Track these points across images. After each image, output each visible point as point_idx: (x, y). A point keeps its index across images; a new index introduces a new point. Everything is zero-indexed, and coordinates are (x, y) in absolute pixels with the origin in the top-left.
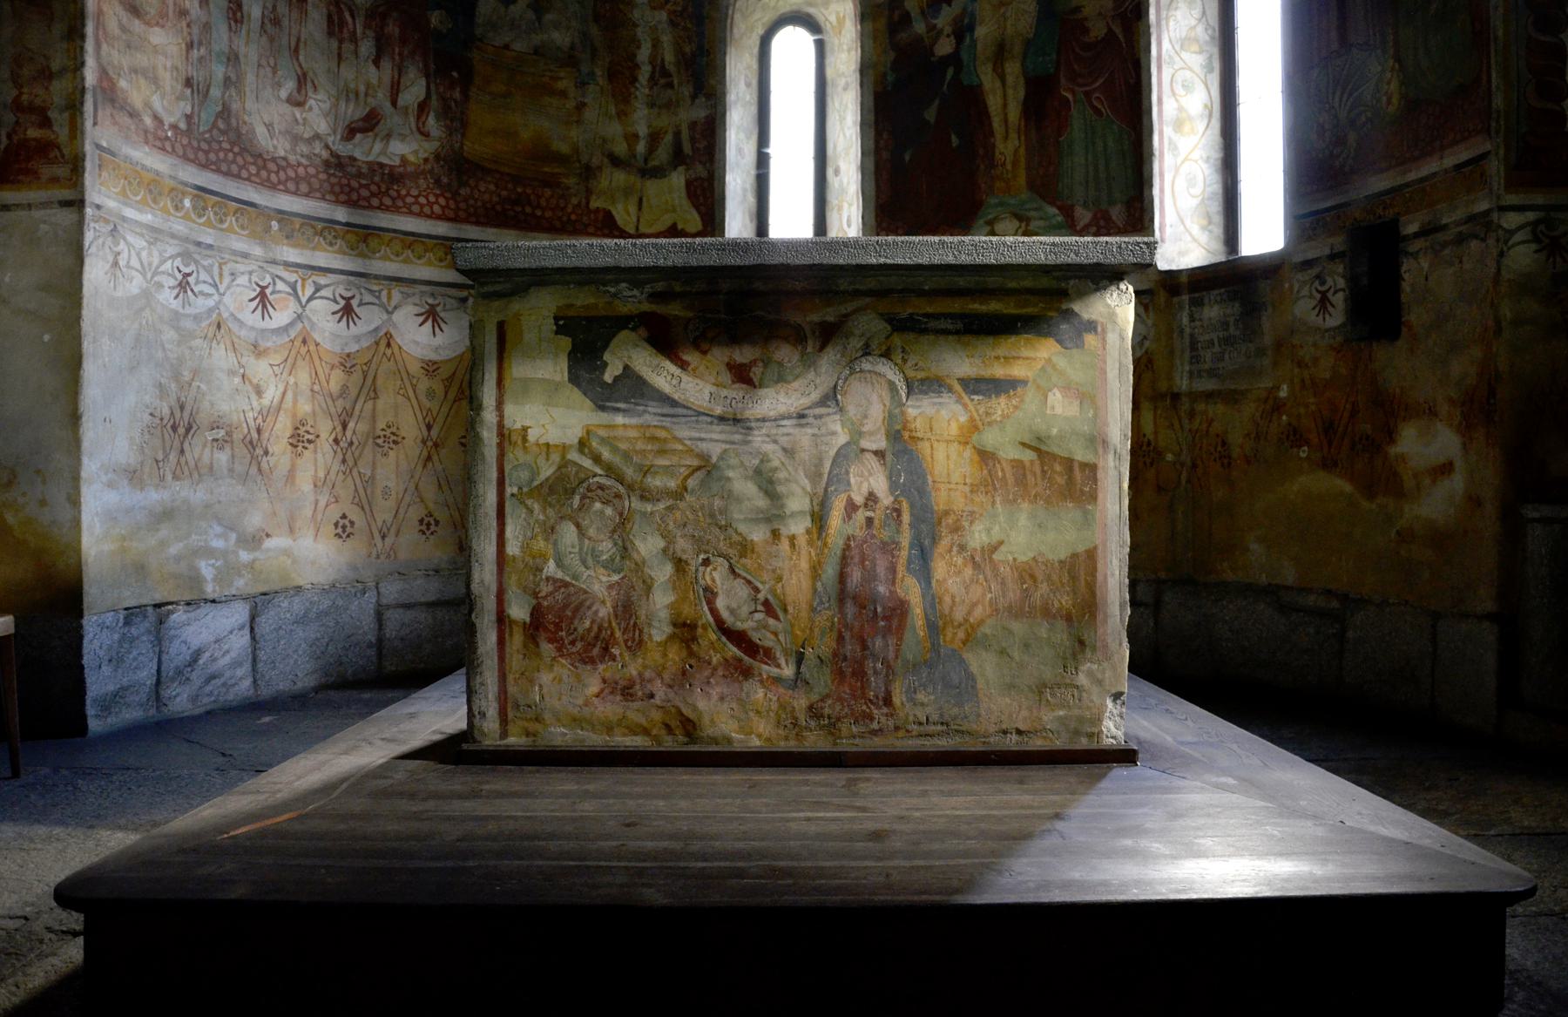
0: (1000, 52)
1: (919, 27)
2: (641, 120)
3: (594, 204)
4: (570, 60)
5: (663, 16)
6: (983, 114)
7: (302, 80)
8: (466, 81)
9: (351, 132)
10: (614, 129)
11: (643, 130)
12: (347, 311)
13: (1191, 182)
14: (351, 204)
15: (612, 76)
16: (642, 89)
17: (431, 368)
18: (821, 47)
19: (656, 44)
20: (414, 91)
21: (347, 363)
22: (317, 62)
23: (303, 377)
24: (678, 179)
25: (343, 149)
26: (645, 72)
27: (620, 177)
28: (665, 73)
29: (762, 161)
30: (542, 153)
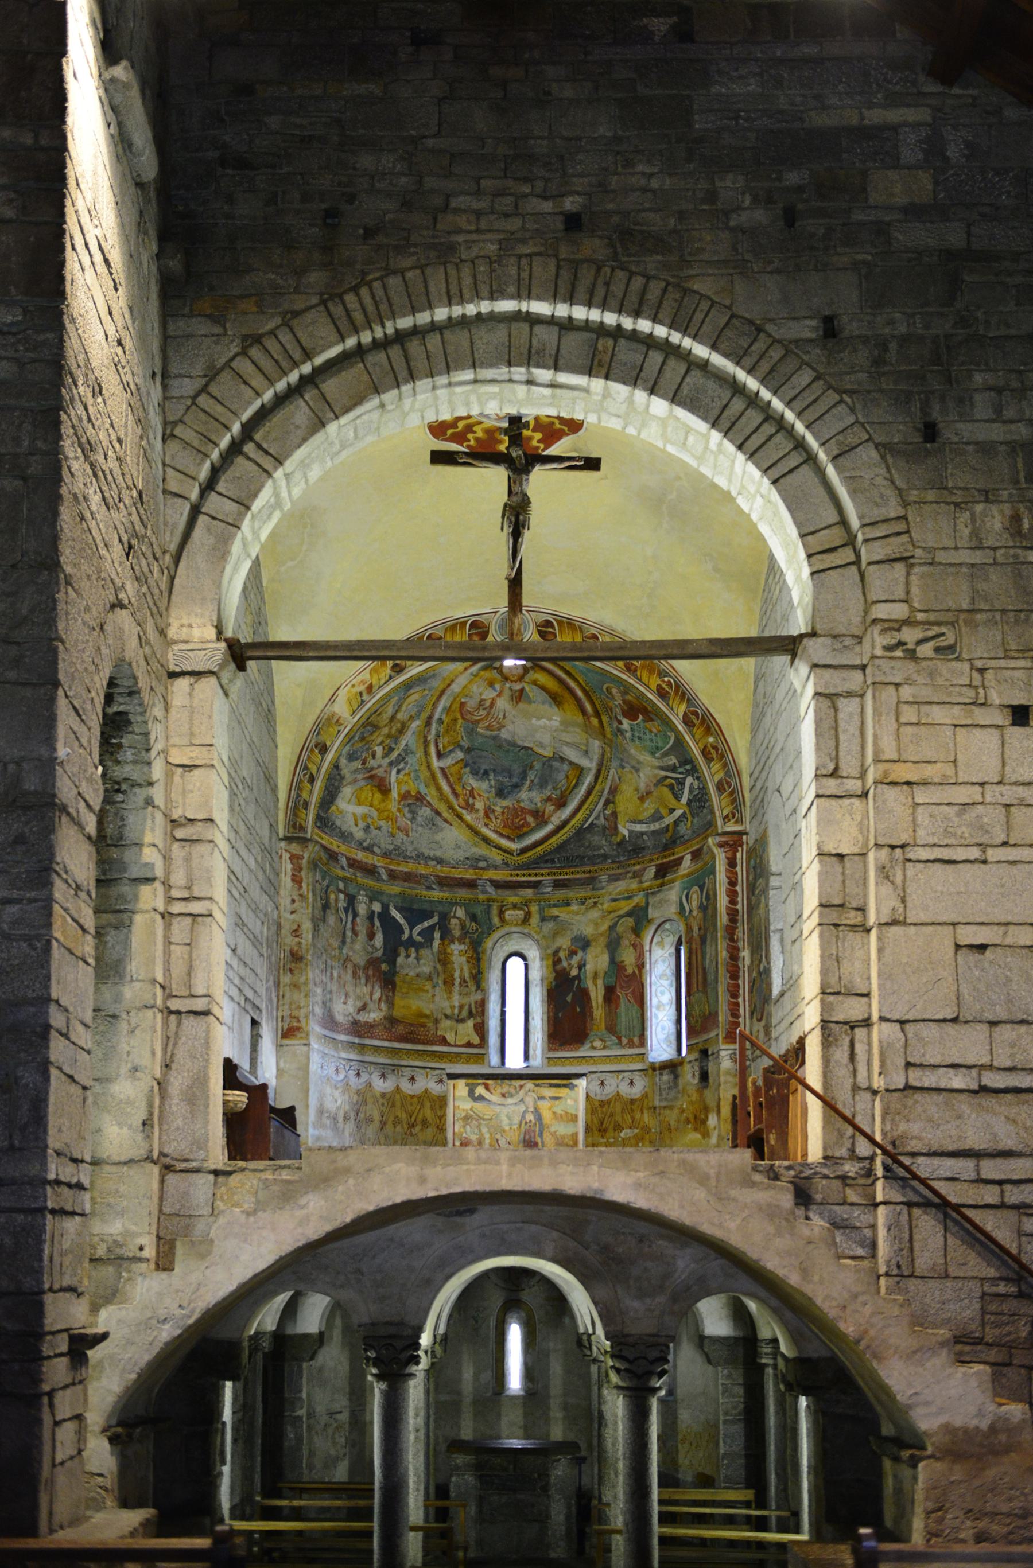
0: (596, 975)
1: (565, 964)
2: (456, 999)
3: (439, 1033)
4: (430, 978)
5: (464, 959)
6: (589, 999)
7: (346, 995)
8: (394, 989)
9: (359, 1011)
10: (446, 1004)
11: (457, 1004)
12: (358, 1074)
13: (663, 1028)
14: (360, 1037)
15: (445, 983)
16: (456, 988)
17: (383, 1095)
18: (526, 966)
19: (462, 970)
20: (377, 995)
21: (358, 1092)
22: (350, 988)
23: (347, 1097)
24: (470, 1023)
25: (357, 1017)
26: (457, 982)
27: (448, 1023)
28: (465, 982)
29: (503, 1013)
30: (421, 1015)
